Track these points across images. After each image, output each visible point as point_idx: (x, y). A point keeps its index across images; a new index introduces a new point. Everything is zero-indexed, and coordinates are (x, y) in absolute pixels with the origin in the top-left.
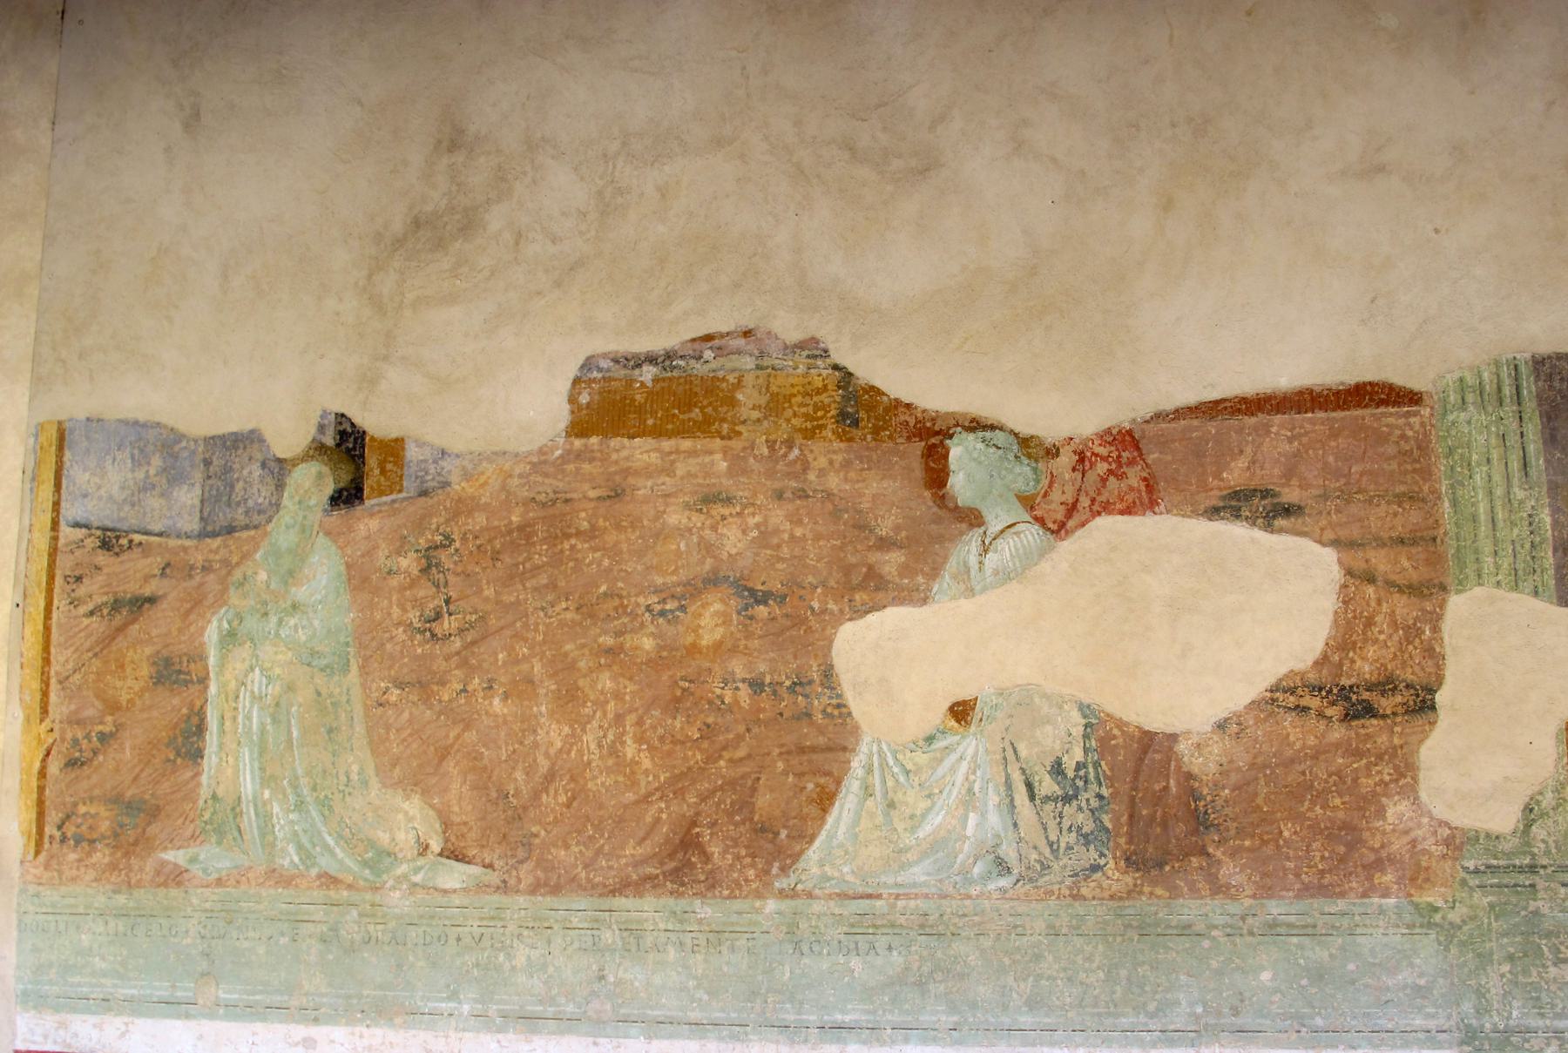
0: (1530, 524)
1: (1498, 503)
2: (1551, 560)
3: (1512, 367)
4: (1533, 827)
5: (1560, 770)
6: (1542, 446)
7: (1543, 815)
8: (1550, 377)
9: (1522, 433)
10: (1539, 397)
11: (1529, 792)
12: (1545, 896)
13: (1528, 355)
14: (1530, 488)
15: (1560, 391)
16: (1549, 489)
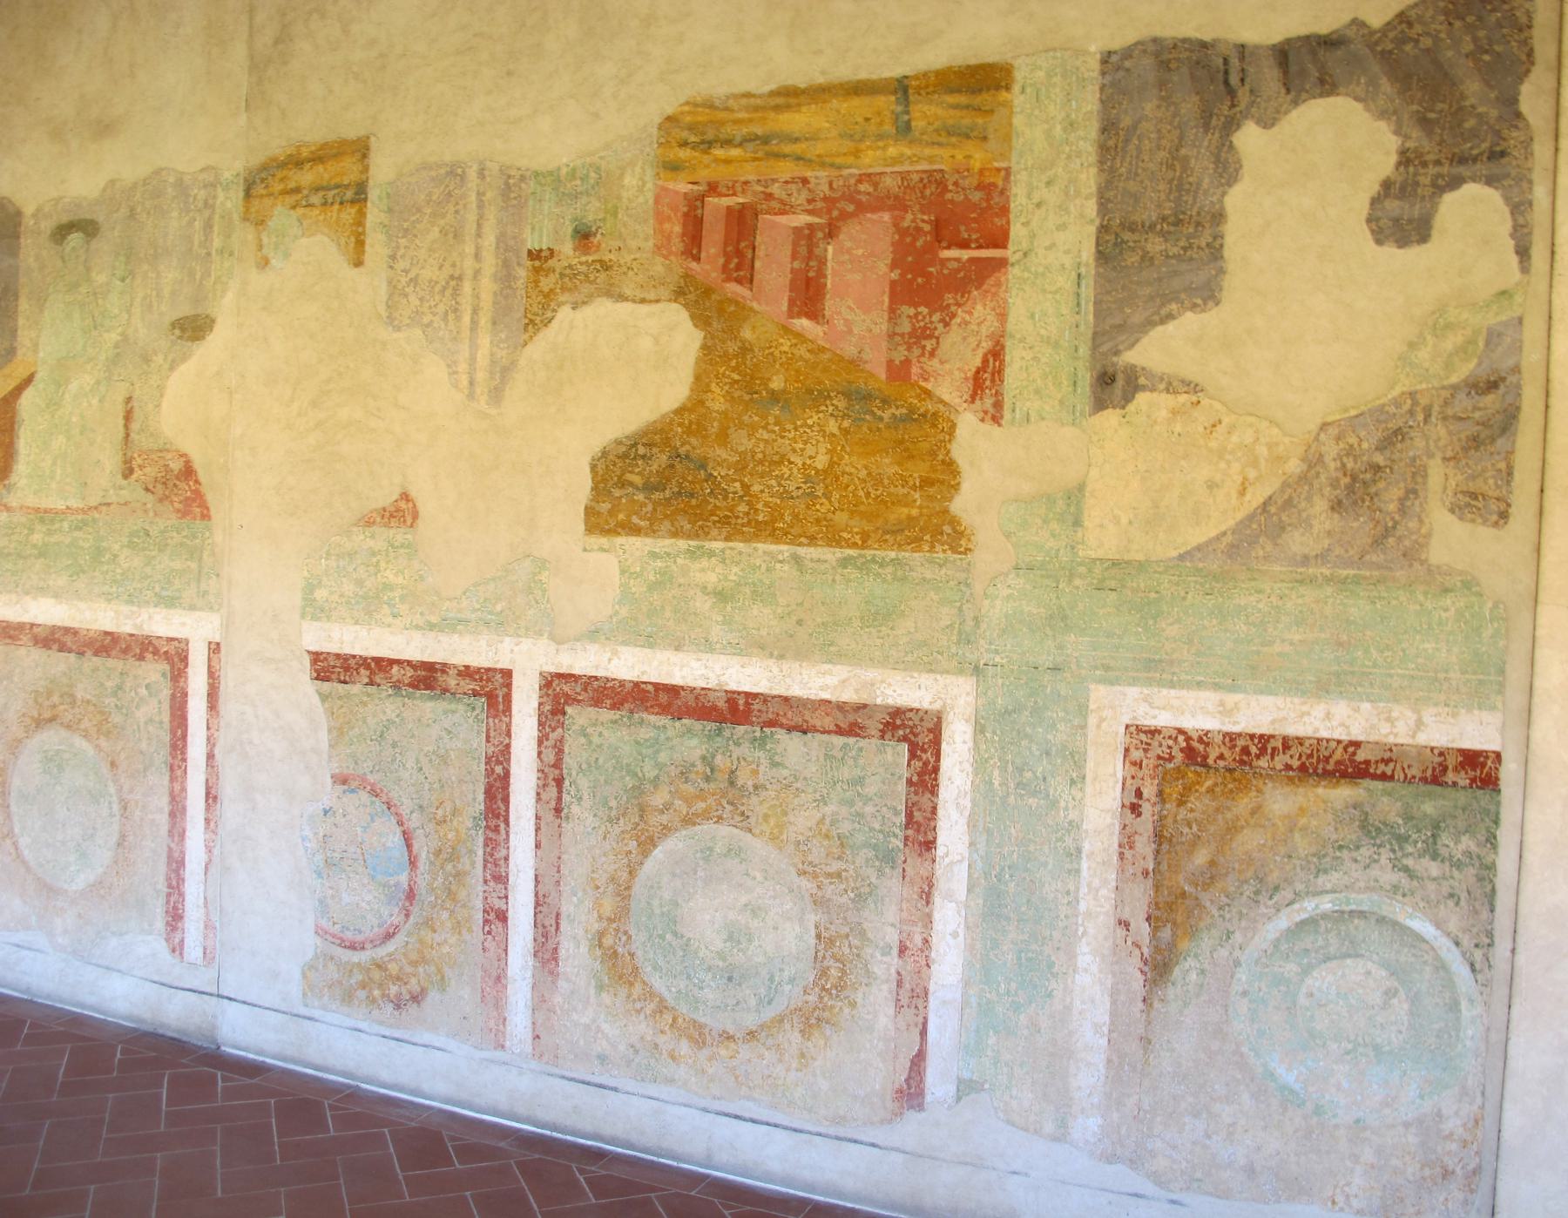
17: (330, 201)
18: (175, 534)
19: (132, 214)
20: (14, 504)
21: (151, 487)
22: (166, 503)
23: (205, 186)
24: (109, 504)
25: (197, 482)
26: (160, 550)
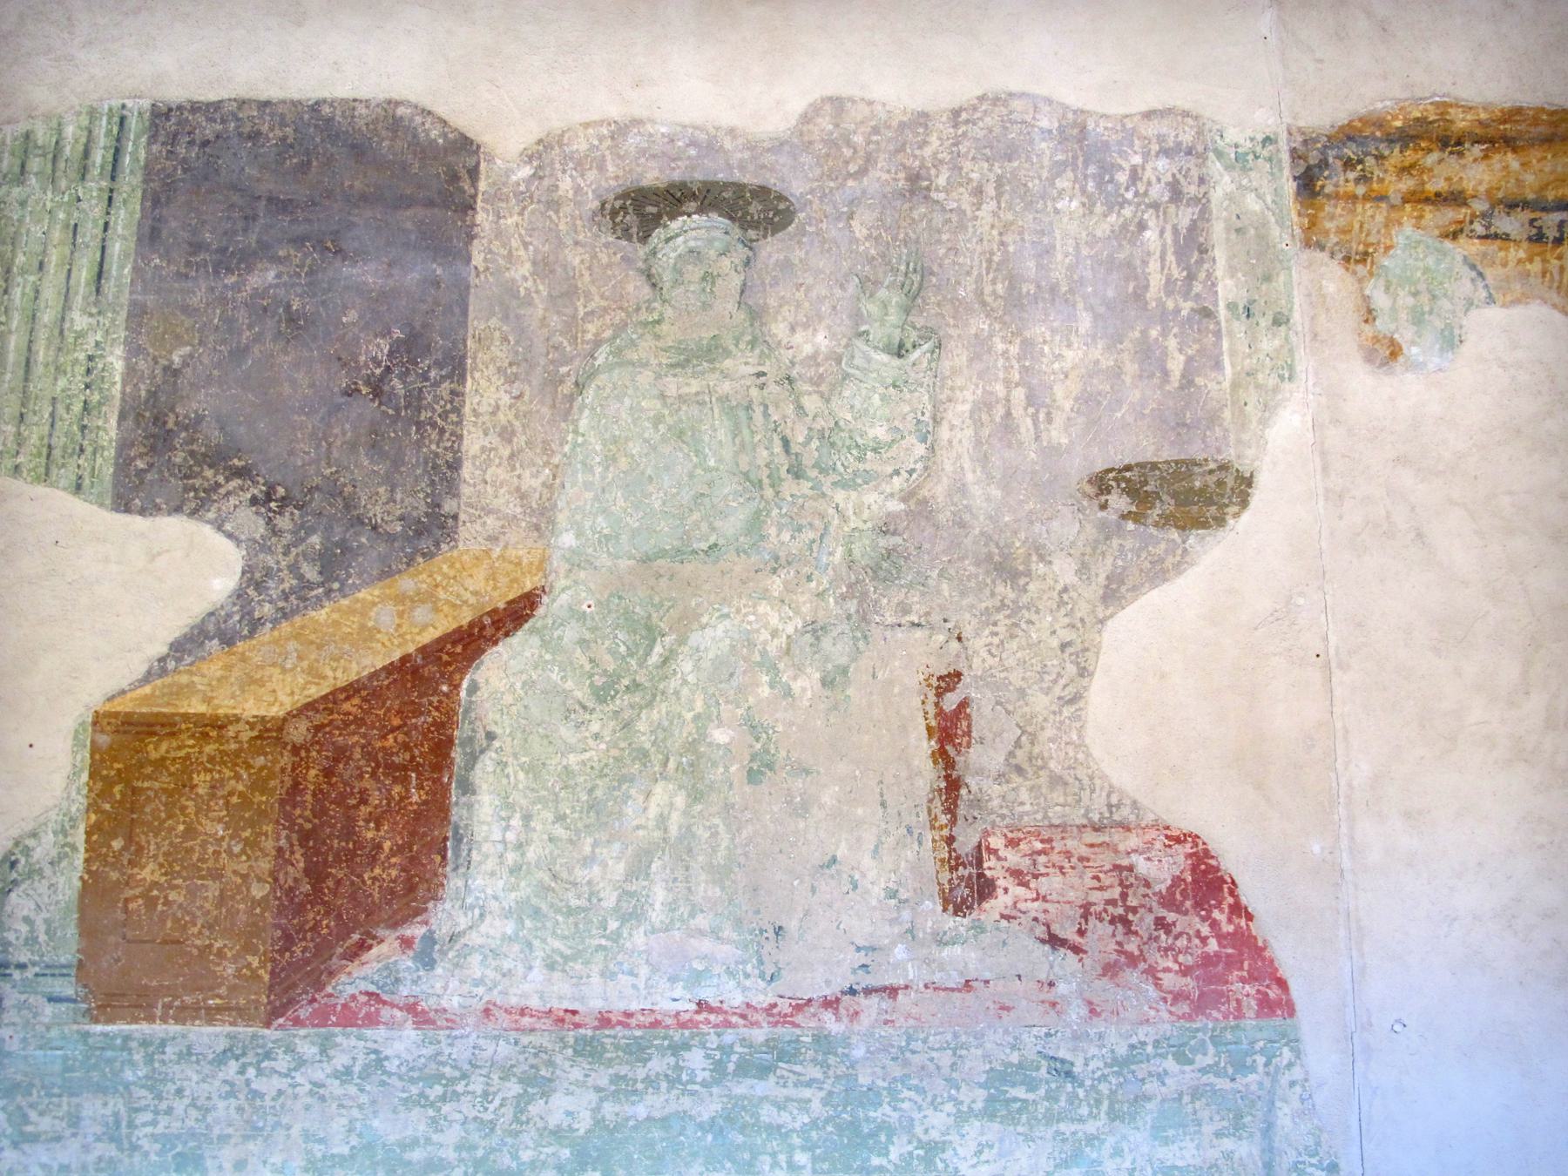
0: (89, 371)
1: (42, 335)
2: (113, 434)
3: (116, 119)
4: (13, 895)
5: (74, 794)
6: (133, 245)
7: (34, 872)
8: (174, 137)
9: (106, 225)
10: (149, 171)
11: (15, 832)
12: (17, 1020)
13: (146, 104)
14: (99, 313)
15: (184, 160)
16: (130, 316)
17: (1552, 233)
18: (1170, 1064)
19: (916, 185)
20: (453, 1002)
21: (1069, 933)
22: (1133, 976)
23: (1166, 152)
24: (892, 991)
25: (1238, 909)
26: (1114, 1116)
